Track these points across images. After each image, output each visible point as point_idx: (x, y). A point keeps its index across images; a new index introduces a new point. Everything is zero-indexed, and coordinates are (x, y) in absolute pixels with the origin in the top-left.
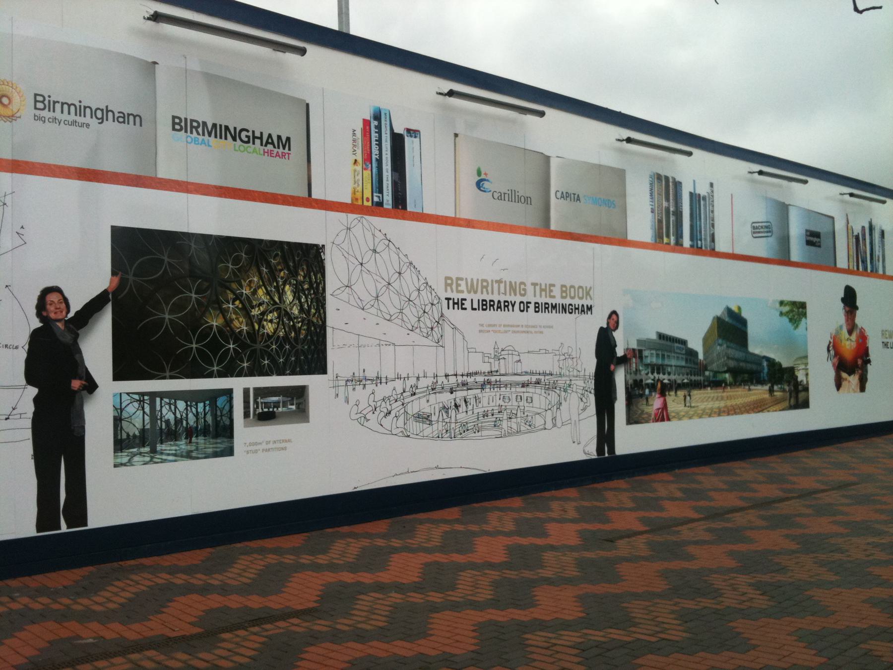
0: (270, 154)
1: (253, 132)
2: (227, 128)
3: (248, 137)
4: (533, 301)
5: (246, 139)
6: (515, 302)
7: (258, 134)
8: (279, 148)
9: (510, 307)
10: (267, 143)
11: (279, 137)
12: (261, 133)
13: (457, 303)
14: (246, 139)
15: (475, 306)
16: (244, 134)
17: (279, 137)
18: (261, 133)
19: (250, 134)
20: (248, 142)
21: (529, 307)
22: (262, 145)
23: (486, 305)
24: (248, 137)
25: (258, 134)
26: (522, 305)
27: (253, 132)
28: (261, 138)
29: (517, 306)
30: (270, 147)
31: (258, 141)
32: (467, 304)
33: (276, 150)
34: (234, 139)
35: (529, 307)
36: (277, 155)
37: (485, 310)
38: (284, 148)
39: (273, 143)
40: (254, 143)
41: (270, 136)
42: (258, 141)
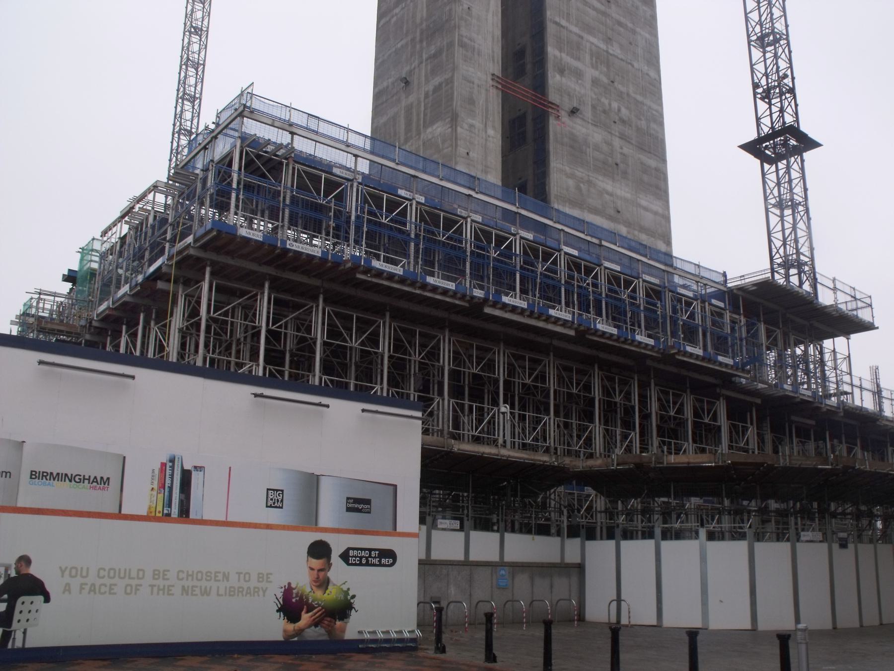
0: (94, 488)
1: (84, 476)
2: (66, 475)
3: (80, 479)
5: (79, 481)
7: (87, 477)
8: (101, 484)
10: (93, 482)
11: (102, 478)
12: (90, 477)
14: (79, 481)
16: (77, 478)
17: (102, 478)
18: (90, 477)
19: (82, 477)
20: (80, 482)
22: (89, 483)
24: (80, 479)
25: (87, 477)
27: (84, 476)
28: (89, 479)
30: (95, 484)
31: (86, 481)
33: (98, 486)
34: (70, 481)
36: (100, 488)
37: (233, 596)
38: (104, 484)
39: (97, 482)
40: (83, 483)
41: (95, 478)
42: (86, 481)
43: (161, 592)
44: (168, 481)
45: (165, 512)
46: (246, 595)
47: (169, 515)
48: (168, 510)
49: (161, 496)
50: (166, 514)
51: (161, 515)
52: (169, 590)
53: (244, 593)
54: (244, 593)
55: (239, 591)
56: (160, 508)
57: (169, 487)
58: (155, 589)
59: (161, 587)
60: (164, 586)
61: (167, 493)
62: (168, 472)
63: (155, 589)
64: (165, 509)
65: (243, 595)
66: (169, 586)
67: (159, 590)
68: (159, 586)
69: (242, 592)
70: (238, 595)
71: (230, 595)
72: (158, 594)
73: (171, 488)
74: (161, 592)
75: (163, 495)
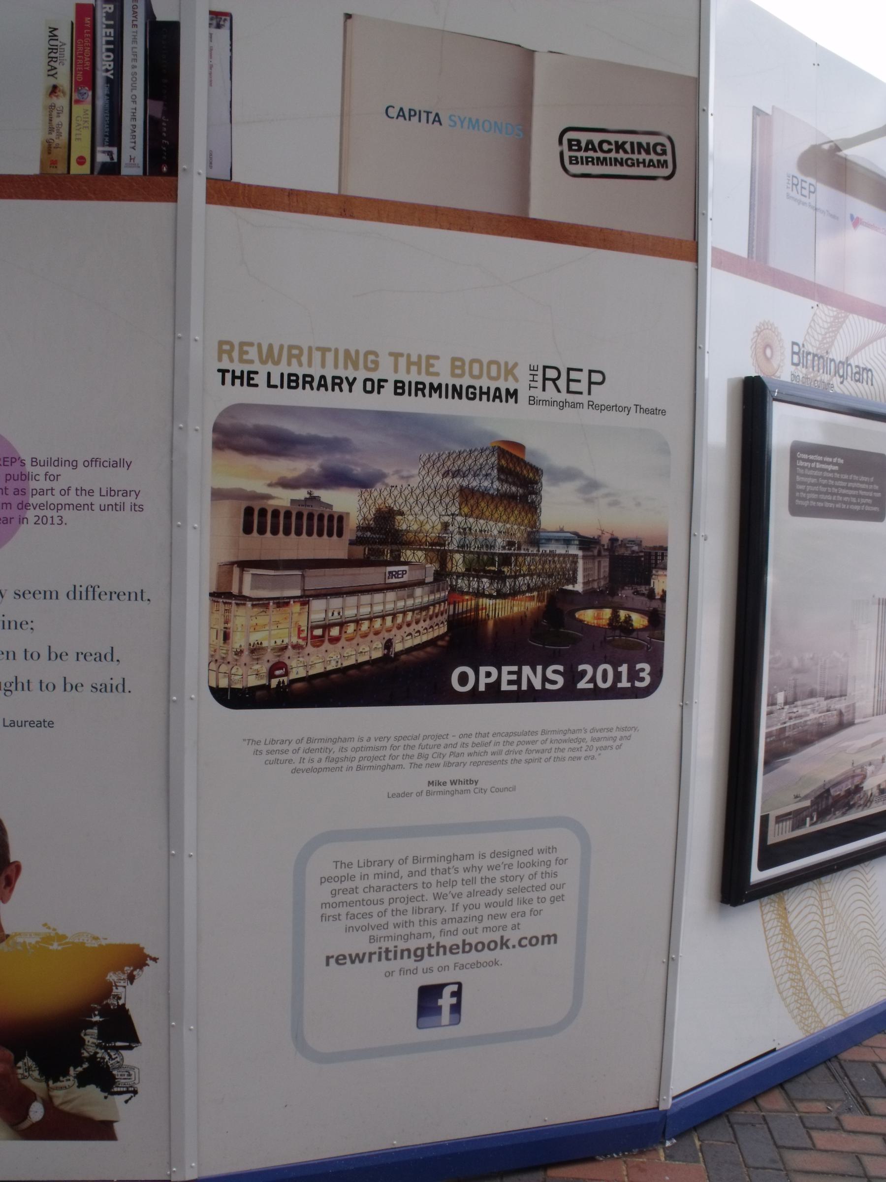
4: (392, 377)
6: (355, 379)
9: (345, 386)
13: (241, 378)
15: (275, 380)
21: (383, 387)
23: (297, 381)
26: (369, 384)
29: (358, 386)
32: (261, 379)
35: (383, 387)
43: (238, 382)
44: (104, 63)
45: (101, 158)
46: (318, 389)
47: (112, 169)
48: (110, 154)
49: (82, 111)
50: (104, 164)
51: (86, 169)
52: (249, 379)
53: (315, 384)
54: (315, 384)
55: (305, 382)
56: (81, 147)
57: (108, 80)
58: (228, 376)
59: (238, 374)
60: (242, 372)
61: (101, 102)
62: (103, 34)
63: (228, 376)
64: (99, 149)
65: (312, 388)
66: (249, 373)
67: (234, 377)
68: (234, 372)
69: (311, 383)
70: (304, 388)
71: (289, 387)
72: (233, 384)
73: (115, 85)
74: (238, 382)
75: (89, 107)
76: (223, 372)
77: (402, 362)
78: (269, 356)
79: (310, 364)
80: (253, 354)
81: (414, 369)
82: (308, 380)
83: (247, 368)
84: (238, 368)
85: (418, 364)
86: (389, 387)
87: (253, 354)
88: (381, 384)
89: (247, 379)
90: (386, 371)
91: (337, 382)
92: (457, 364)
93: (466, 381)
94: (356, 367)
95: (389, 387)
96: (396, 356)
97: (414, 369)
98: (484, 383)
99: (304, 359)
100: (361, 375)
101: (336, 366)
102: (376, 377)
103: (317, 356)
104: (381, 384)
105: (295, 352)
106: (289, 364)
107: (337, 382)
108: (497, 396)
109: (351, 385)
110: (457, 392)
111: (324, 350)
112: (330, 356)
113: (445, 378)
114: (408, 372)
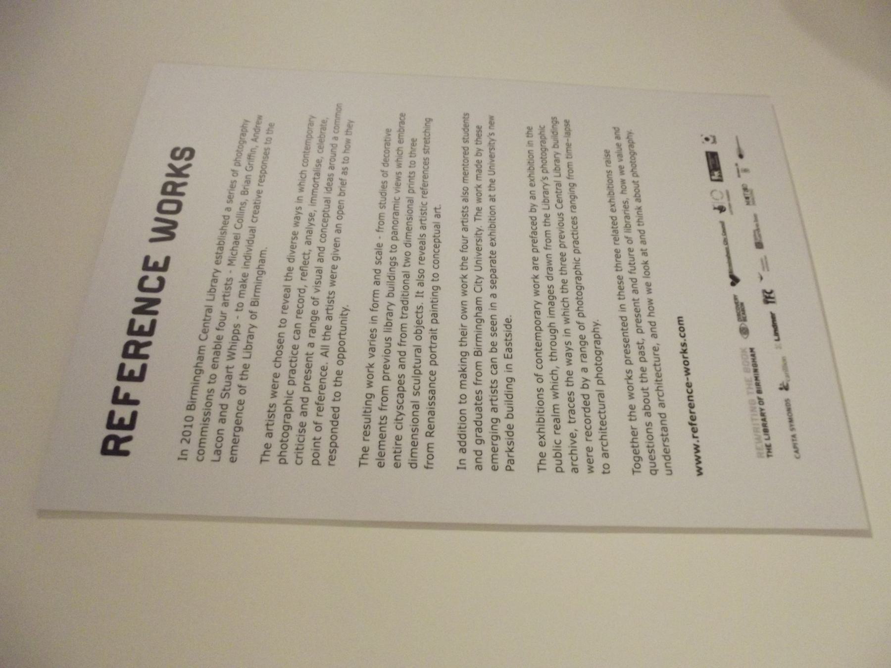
29: (762, 407)
32: (768, 442)
76: (768, 456)
77: (751, 391)
78: (758, 439)
79: (758, 424)
80: (759, 445)
81: (751, 386)
82: (764, 425)
83: (765, 447)
84: (765, 451)
85: (750, 385)
86: (760, 396)
87: (759, 445)
88: (759, 399)
89: (769, 447)
90: (755, 396)
91: (763, 415)
92: (746, 371)
93: (752, 368)
94: (755, 408)
95: (760, 396)
96: (748, 393)
97: (751, 386)
98: (750, 360)
99: (757, 426)
100: (758, 406)
101: (756, 415)
102: (757, 401)
103: (755, 422)
104: (759, 399)
105: (756, 430)
106: (759, 432)
107: (763, 415)
108: (753, 355)
109: (762, 410)
110: (756, 371)
111: (752, 420)
112: (755, 417)
113: (751, 375)
114: (752, 388)
